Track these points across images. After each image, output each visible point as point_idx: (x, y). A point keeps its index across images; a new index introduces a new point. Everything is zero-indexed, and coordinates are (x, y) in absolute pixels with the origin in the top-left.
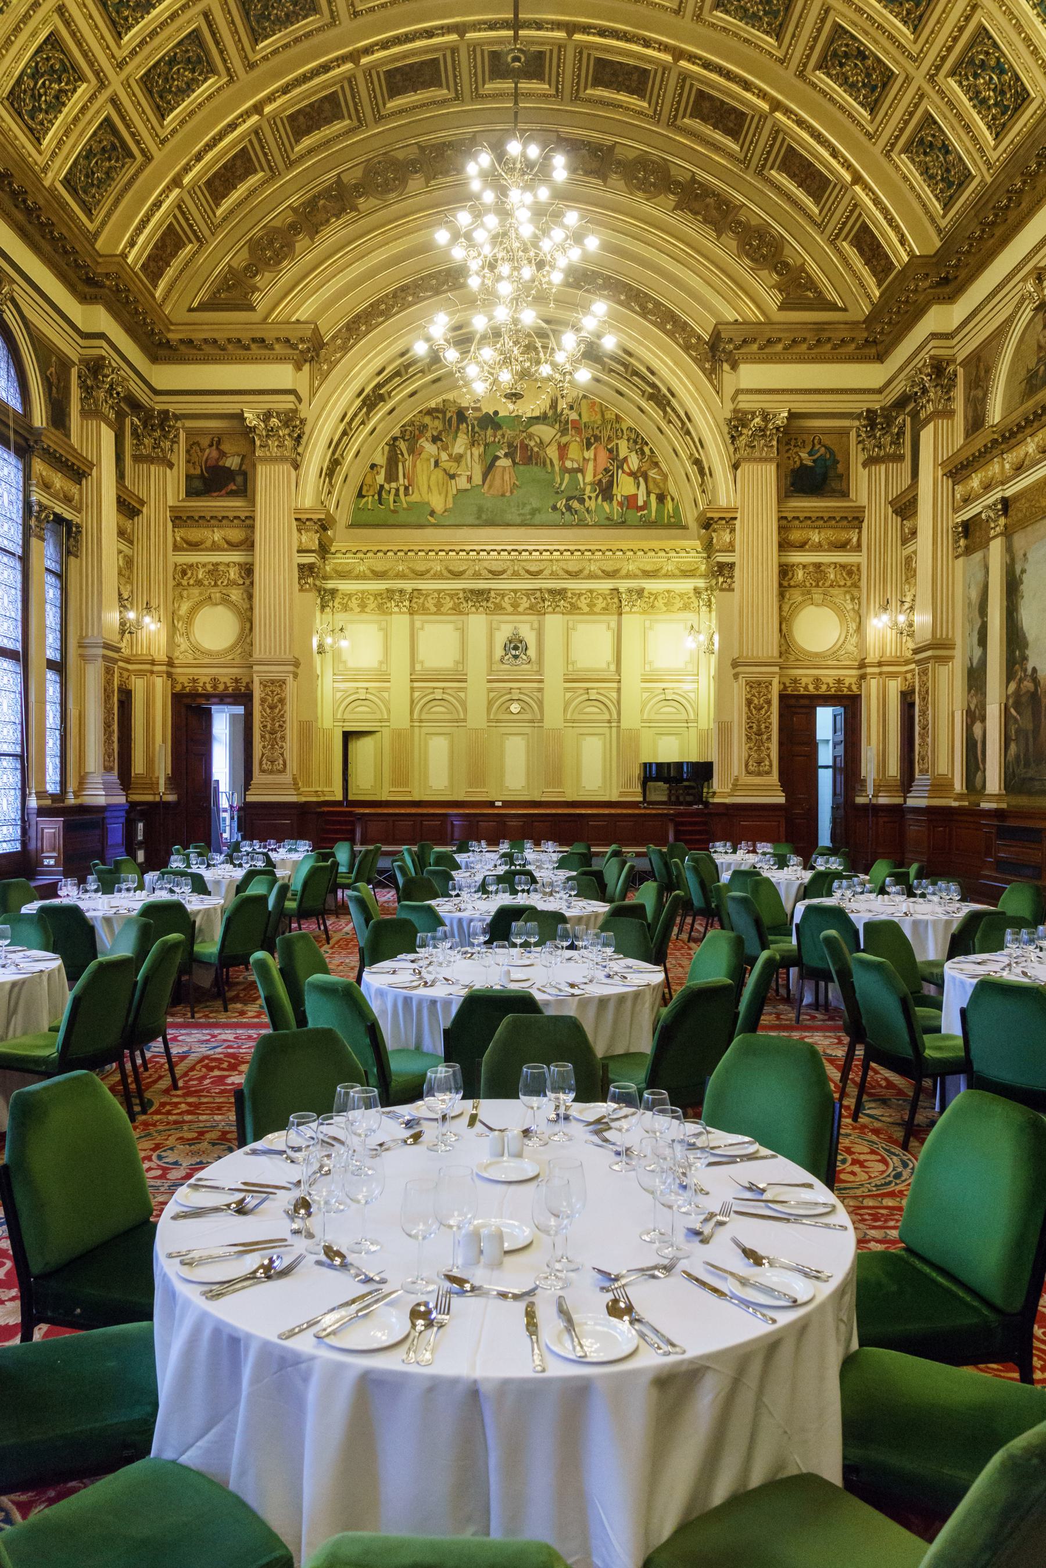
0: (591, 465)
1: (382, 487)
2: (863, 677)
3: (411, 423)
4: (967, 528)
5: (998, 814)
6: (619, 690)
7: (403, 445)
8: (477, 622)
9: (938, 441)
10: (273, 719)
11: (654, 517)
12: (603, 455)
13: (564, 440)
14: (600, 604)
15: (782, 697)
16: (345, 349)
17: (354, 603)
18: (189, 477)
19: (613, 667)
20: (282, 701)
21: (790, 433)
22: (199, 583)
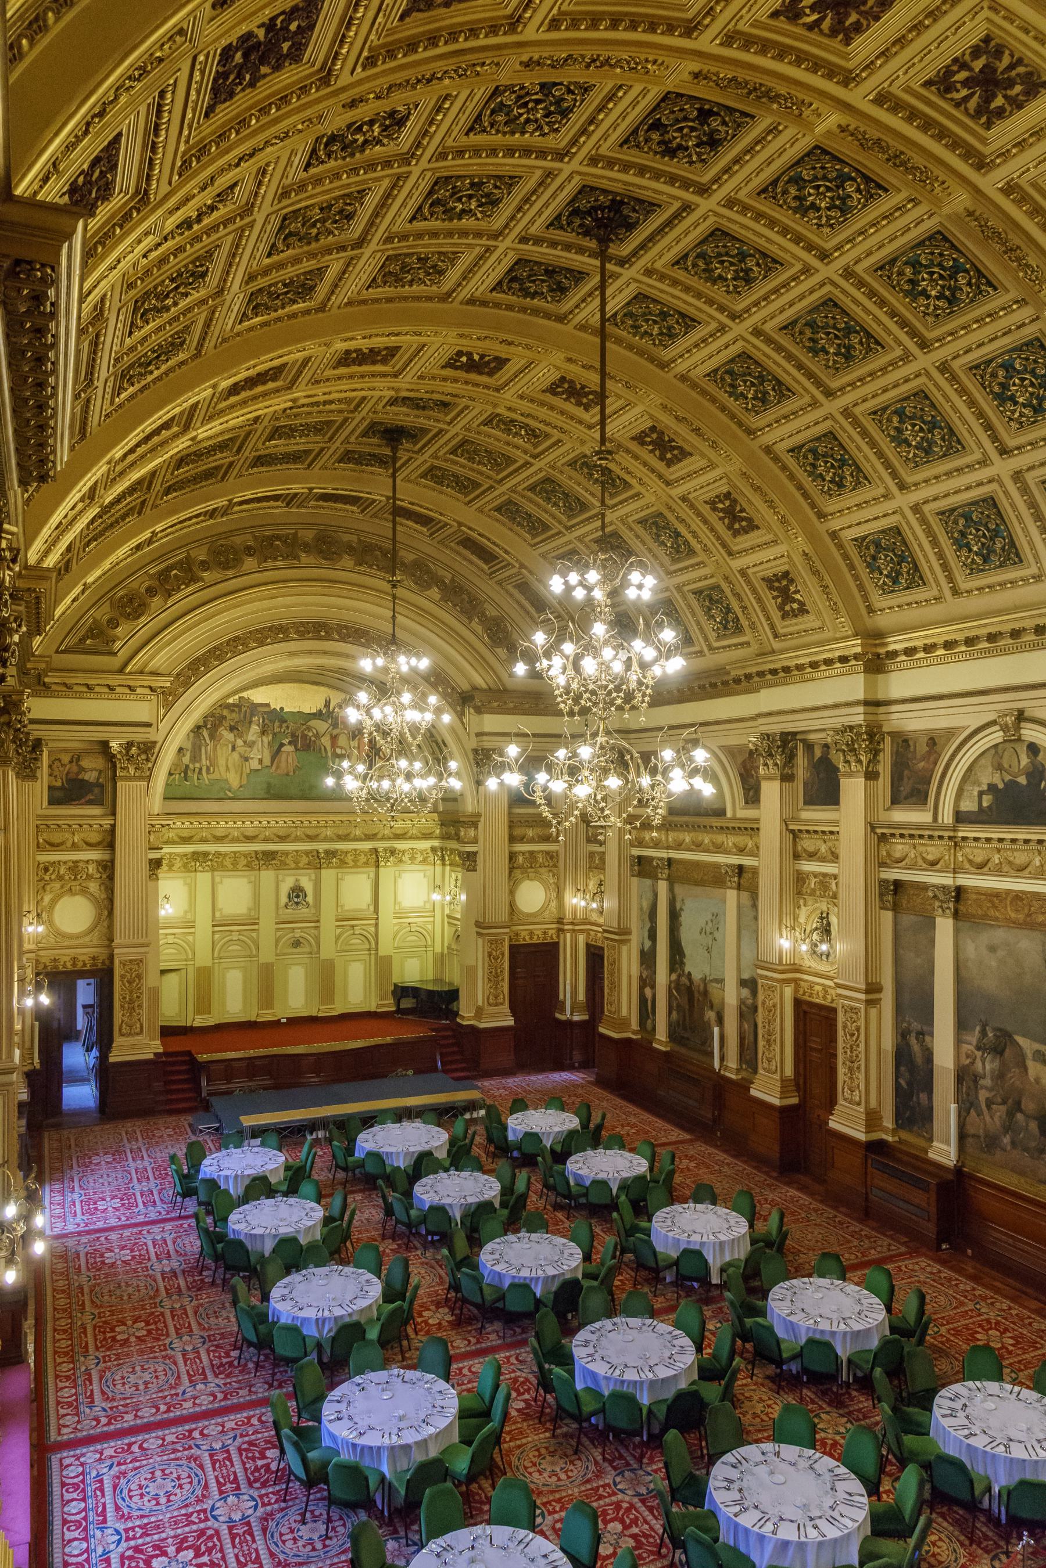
2: (560, 930)
3: (212, 715)
7: (205, 733)
8: (267, 876)
14: (363, 859)
15: (511, 947)
18: (50, 788)
22: (60, 878)
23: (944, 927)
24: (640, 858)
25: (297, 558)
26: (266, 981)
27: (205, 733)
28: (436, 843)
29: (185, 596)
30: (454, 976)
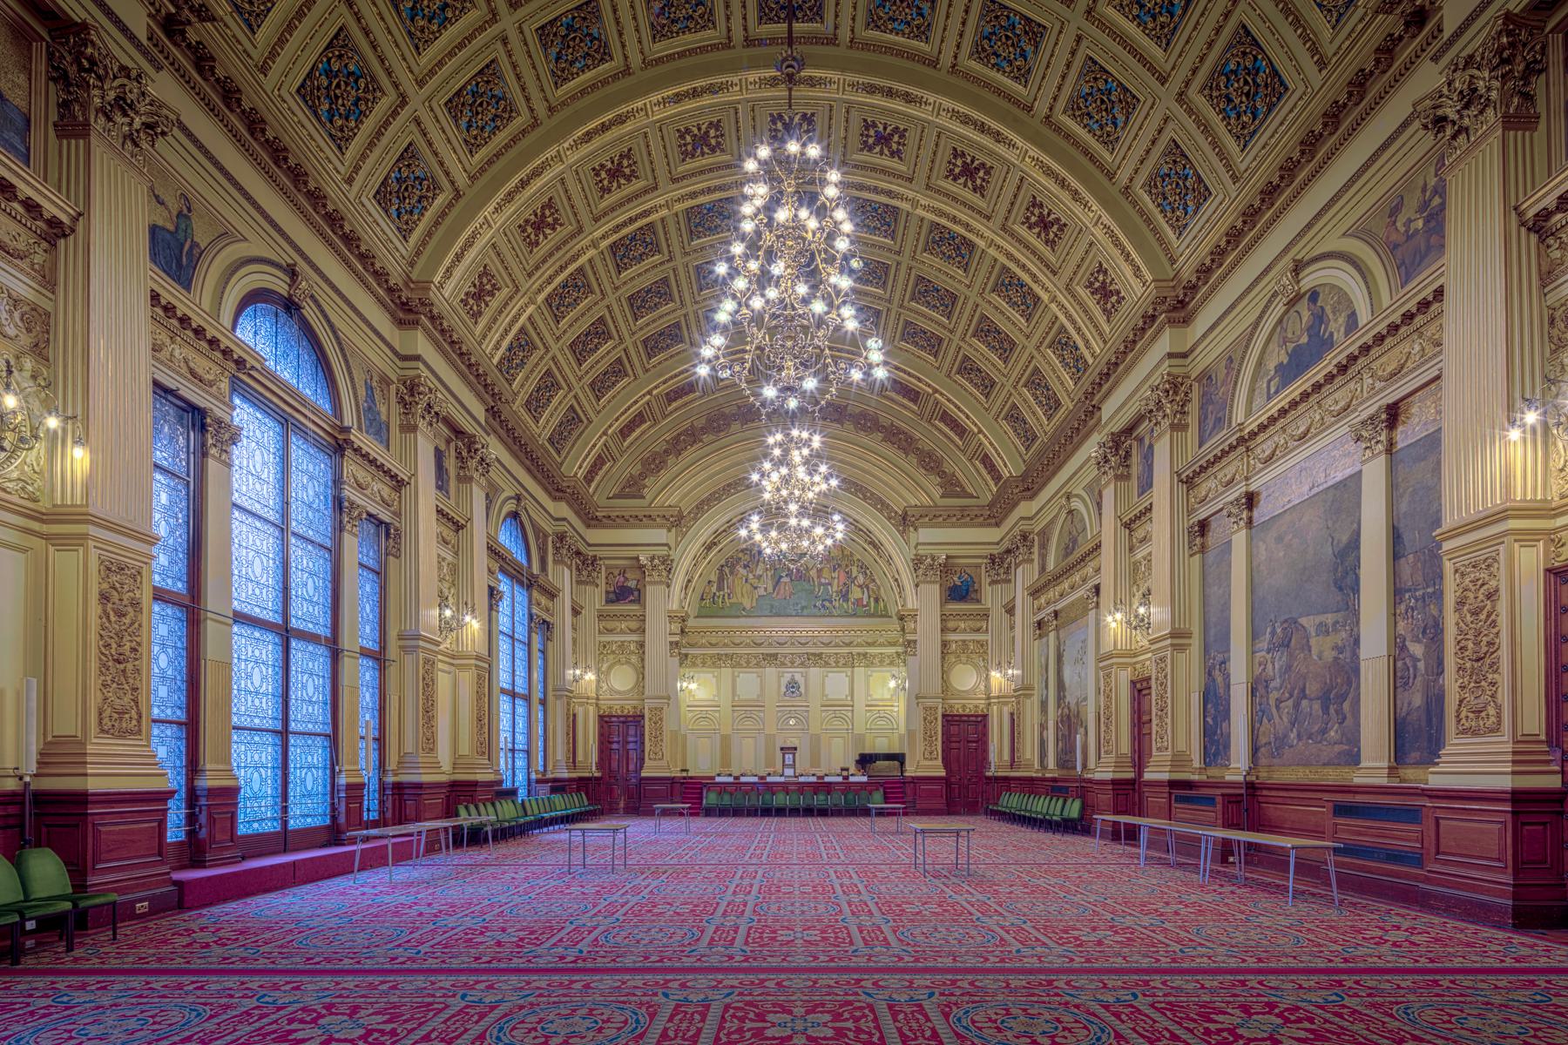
0: (836, 581)
4: (1040, 624)
5: (1054, 780)
7: (727, 570)
8: (771, 672)
9: (1025, 575)
11: (874, 609)
12: (843, 574)
14: (842, 661)
16: (696, 519)
17: (699, 661)
18: (607, 592)
21: (947, 568)
27: (727, 570)
28: (900, 650)
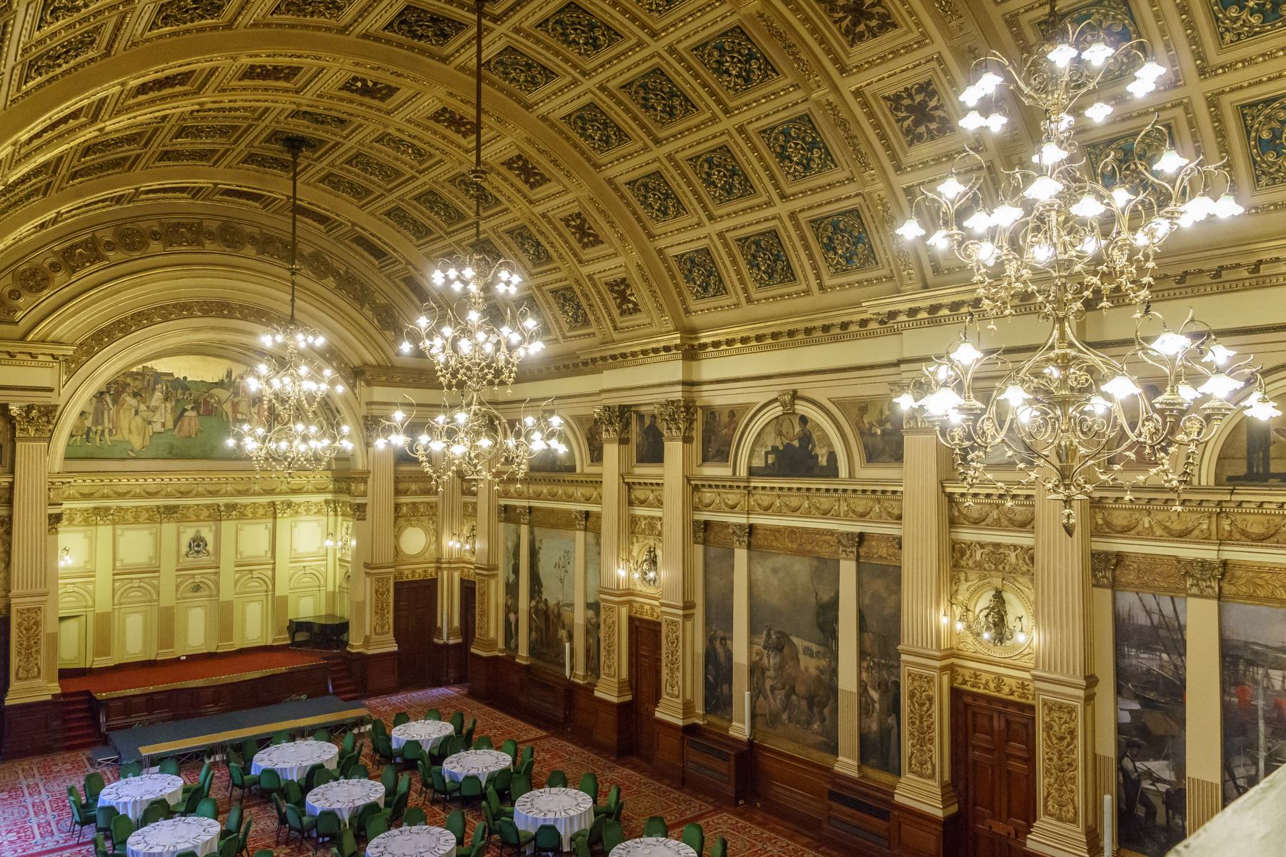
1: (89, 429)
3: (116, 382)
6: (274, 569)
7: (108, 398)
8: (169, 528)
10: (28, 639)
13: (236, 400)
14: (261, 511)
15: (396, 584)
19: (269, 554)
20: (37, 623)
23: (741, 555)
24: (506, 506)
25: (201, 244)
26: (167, 624)
27: (108, 398)
28: (329, 497)
29: (90, 274)
30: (344, 611)
